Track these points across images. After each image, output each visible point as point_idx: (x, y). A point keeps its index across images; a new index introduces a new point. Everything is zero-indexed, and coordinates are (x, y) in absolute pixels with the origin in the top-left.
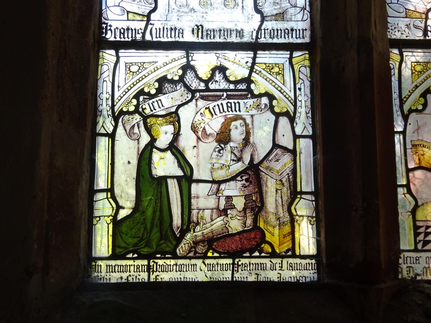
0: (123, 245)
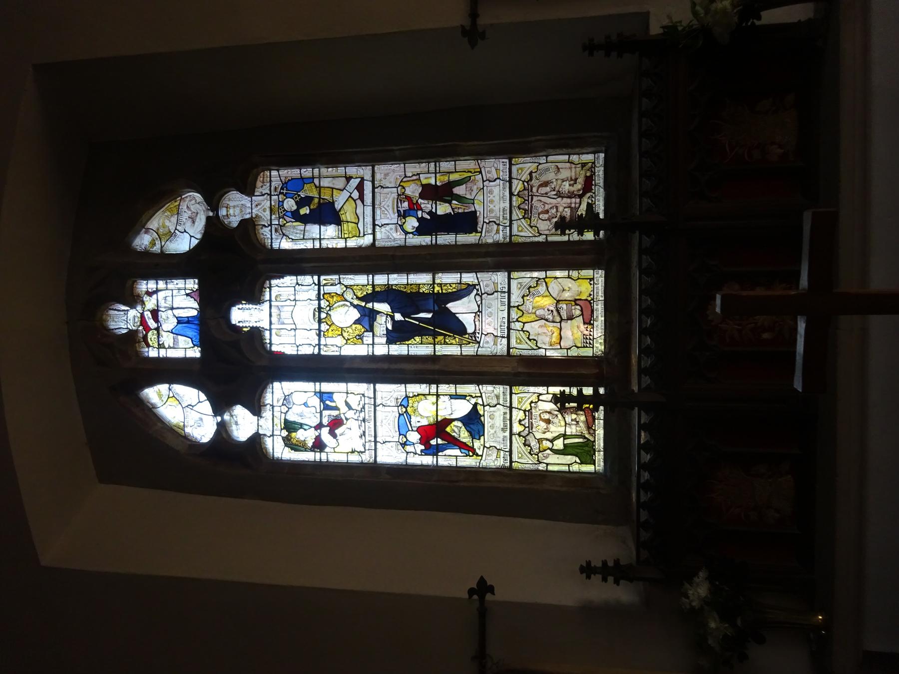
0: (590, 461)
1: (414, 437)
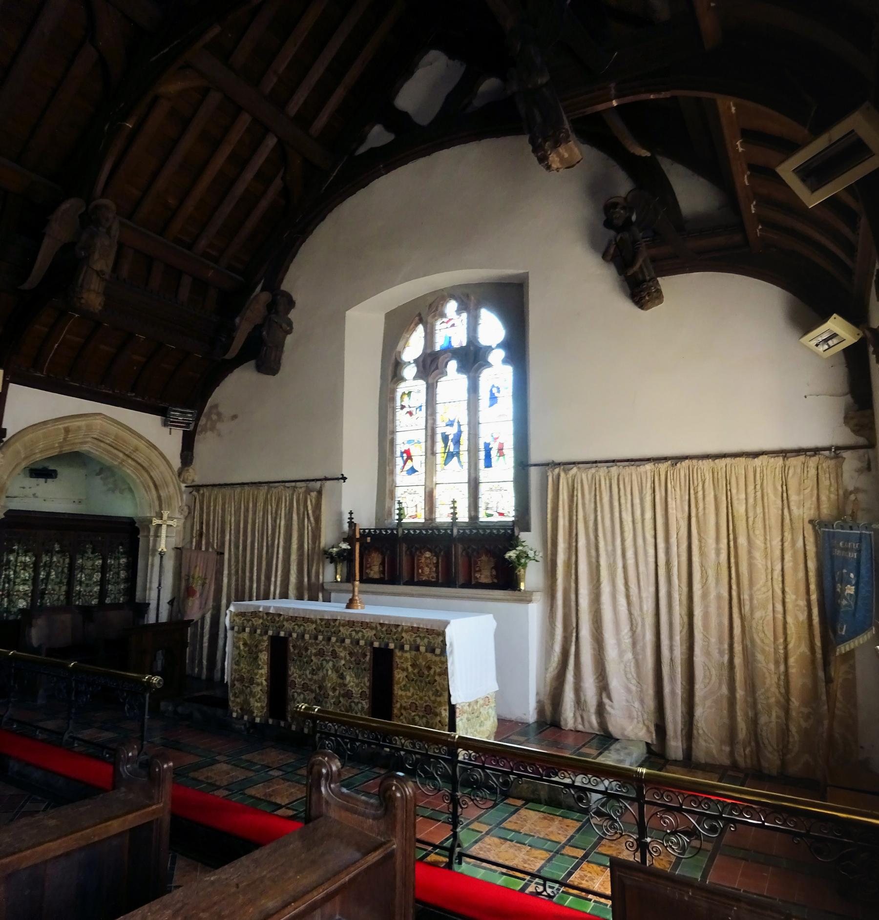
1: (406, 447)
